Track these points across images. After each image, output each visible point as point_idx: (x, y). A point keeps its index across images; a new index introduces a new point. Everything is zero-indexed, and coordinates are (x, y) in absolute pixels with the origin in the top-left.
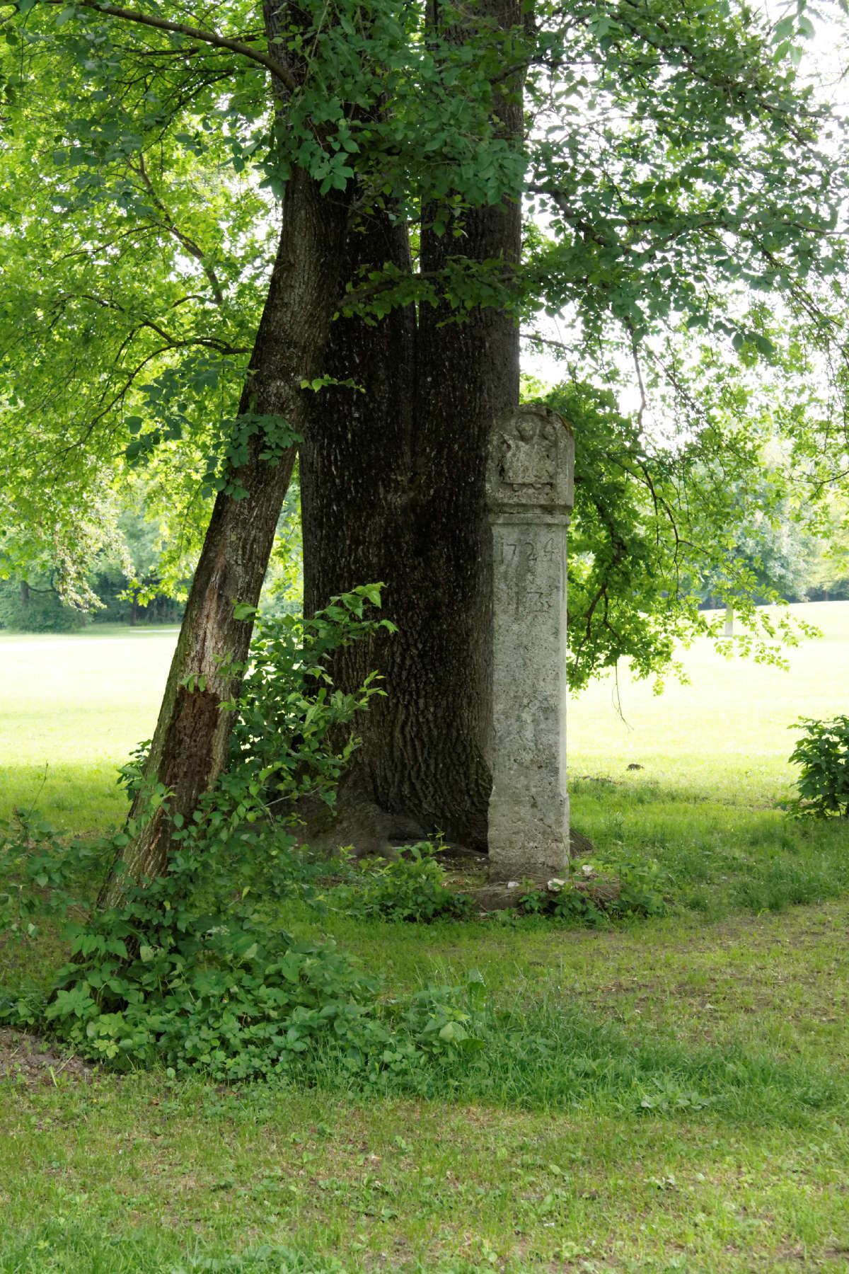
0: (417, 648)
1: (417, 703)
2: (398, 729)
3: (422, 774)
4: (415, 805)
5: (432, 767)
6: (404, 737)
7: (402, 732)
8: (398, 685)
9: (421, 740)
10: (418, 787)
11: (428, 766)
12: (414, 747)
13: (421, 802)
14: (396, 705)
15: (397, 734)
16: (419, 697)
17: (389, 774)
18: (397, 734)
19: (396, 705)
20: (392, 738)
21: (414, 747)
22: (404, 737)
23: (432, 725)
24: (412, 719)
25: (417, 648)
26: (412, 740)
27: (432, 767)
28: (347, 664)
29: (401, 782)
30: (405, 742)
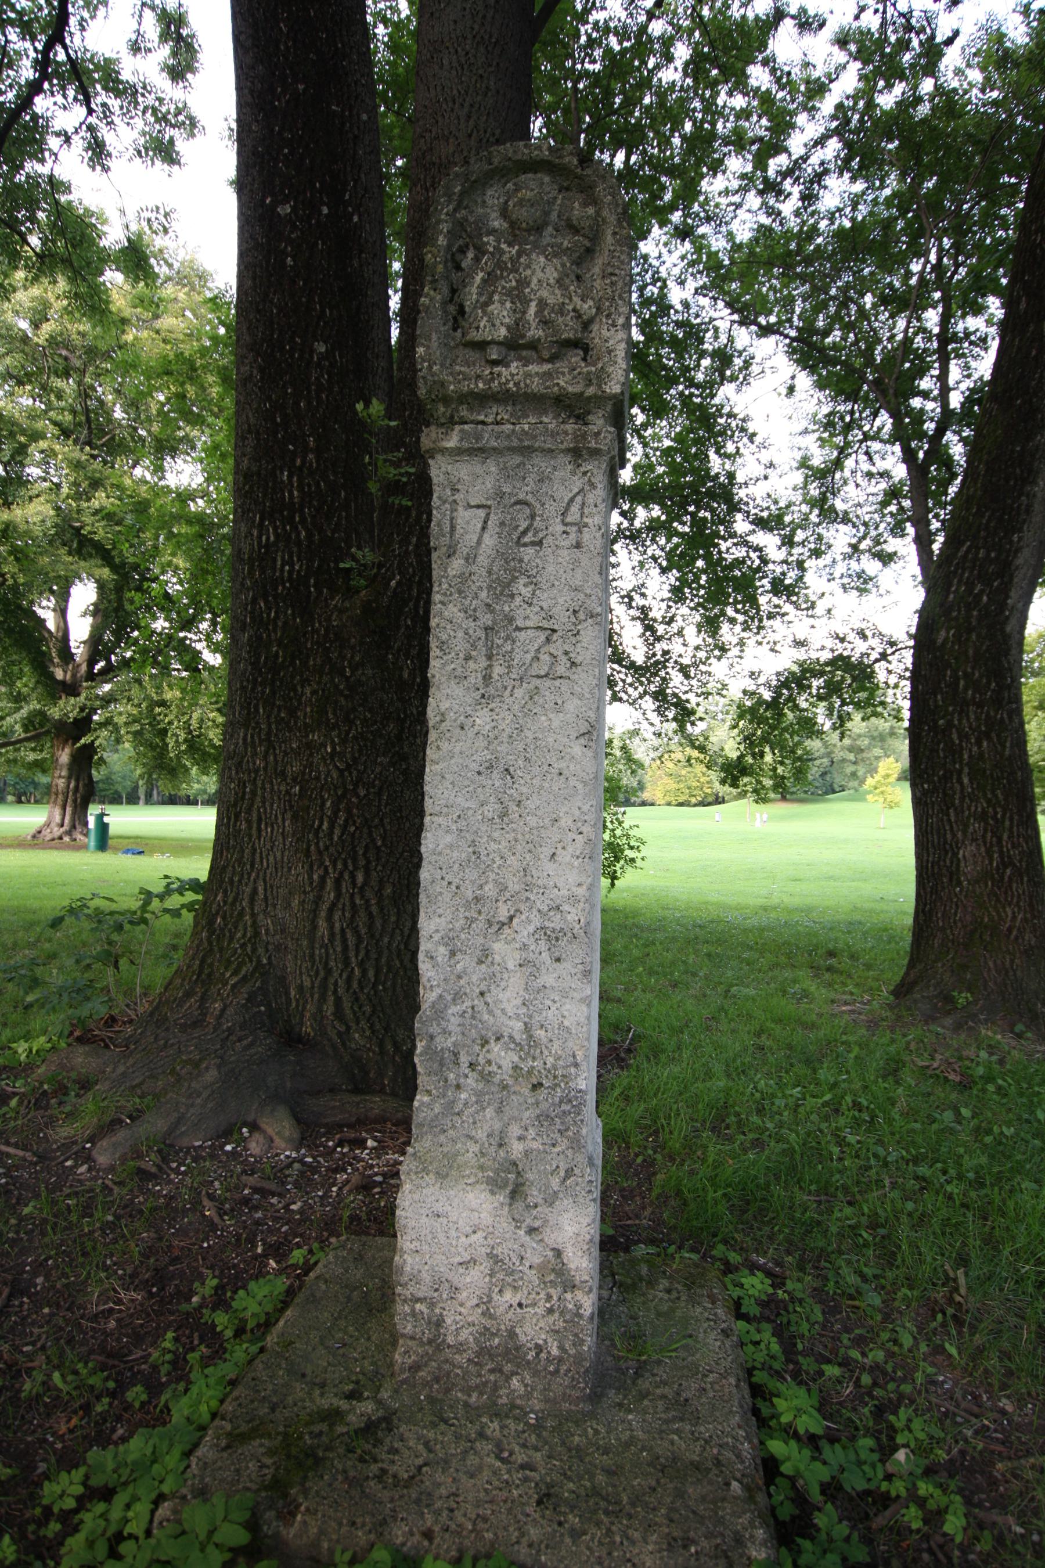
0: (358, 796)
1: (353, 877)
2: (323, 914)
3: (355, 985)
4: (340, 1034)
5: (371, 973)
6: (331, 927)
7: (329, 918)
8: (327, 848)
9: (356, 932)
10: (346, 1005)
11: (364, 972)
12: (344, 940)
13: (348, 1028)
14: (323, 880)
15: (322, 924)
16: (356, 868)
17: (307, 983)
18: (322, 924)
19: (323, 880)
20: (315, 927)
21: (344, 940)
22: (331, 927)
23: (374, 909)
24: (345, 899)
25: (358, 796)
26: (343, 930)
27: (371, 973)
28: (260, 820)
29: (323, 998)
30: (332, 935)
